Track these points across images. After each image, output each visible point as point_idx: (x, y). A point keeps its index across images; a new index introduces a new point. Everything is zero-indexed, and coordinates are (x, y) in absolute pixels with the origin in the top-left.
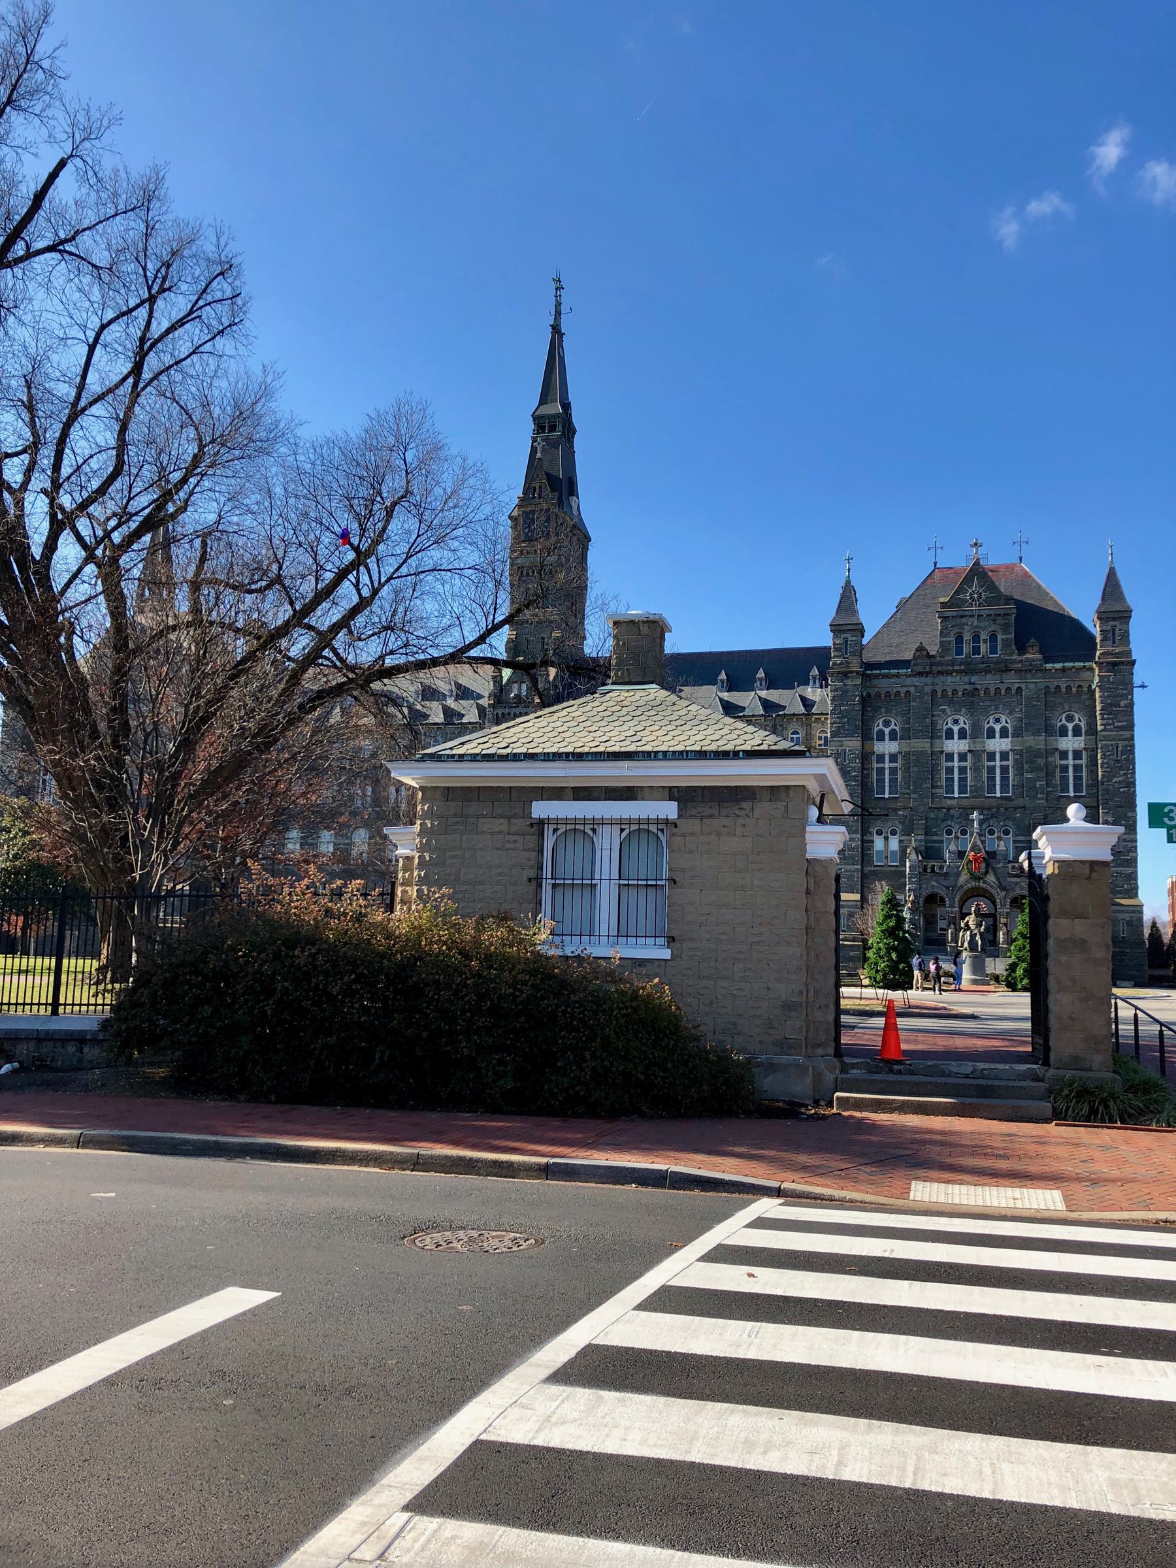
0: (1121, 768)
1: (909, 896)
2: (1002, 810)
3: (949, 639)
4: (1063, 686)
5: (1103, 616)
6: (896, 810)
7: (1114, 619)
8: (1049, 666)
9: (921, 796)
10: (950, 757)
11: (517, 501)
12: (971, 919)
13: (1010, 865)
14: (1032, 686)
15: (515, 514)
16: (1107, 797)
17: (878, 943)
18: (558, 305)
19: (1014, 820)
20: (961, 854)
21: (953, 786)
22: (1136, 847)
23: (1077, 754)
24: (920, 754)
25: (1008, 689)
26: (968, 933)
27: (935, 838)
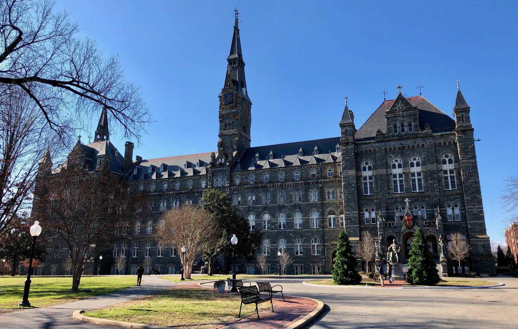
0: (472, 176)
1: (380, 237)
2: (420, 198)
3: (390, 126)
4: (442, 142)
5: (457, 111)
6: (373, 200)
7: (462, 112)
8: (435, 134)
9: (383, 194)
10: (395, 176)
11: (221, 91)
12: (393, 246)
13: (424, 222)
14: (429, 143)
15: (221, 95)
16: (467, 189)
17: (338, 260)
18: (237, 20)
19: (425, 202)
20: (402, 218)
21: (397, 188)
22: (483, 211)
23: (451, 172)
24: (381, 175)
25: (418, 146)
26: (391, 253)
27: (391, 211)
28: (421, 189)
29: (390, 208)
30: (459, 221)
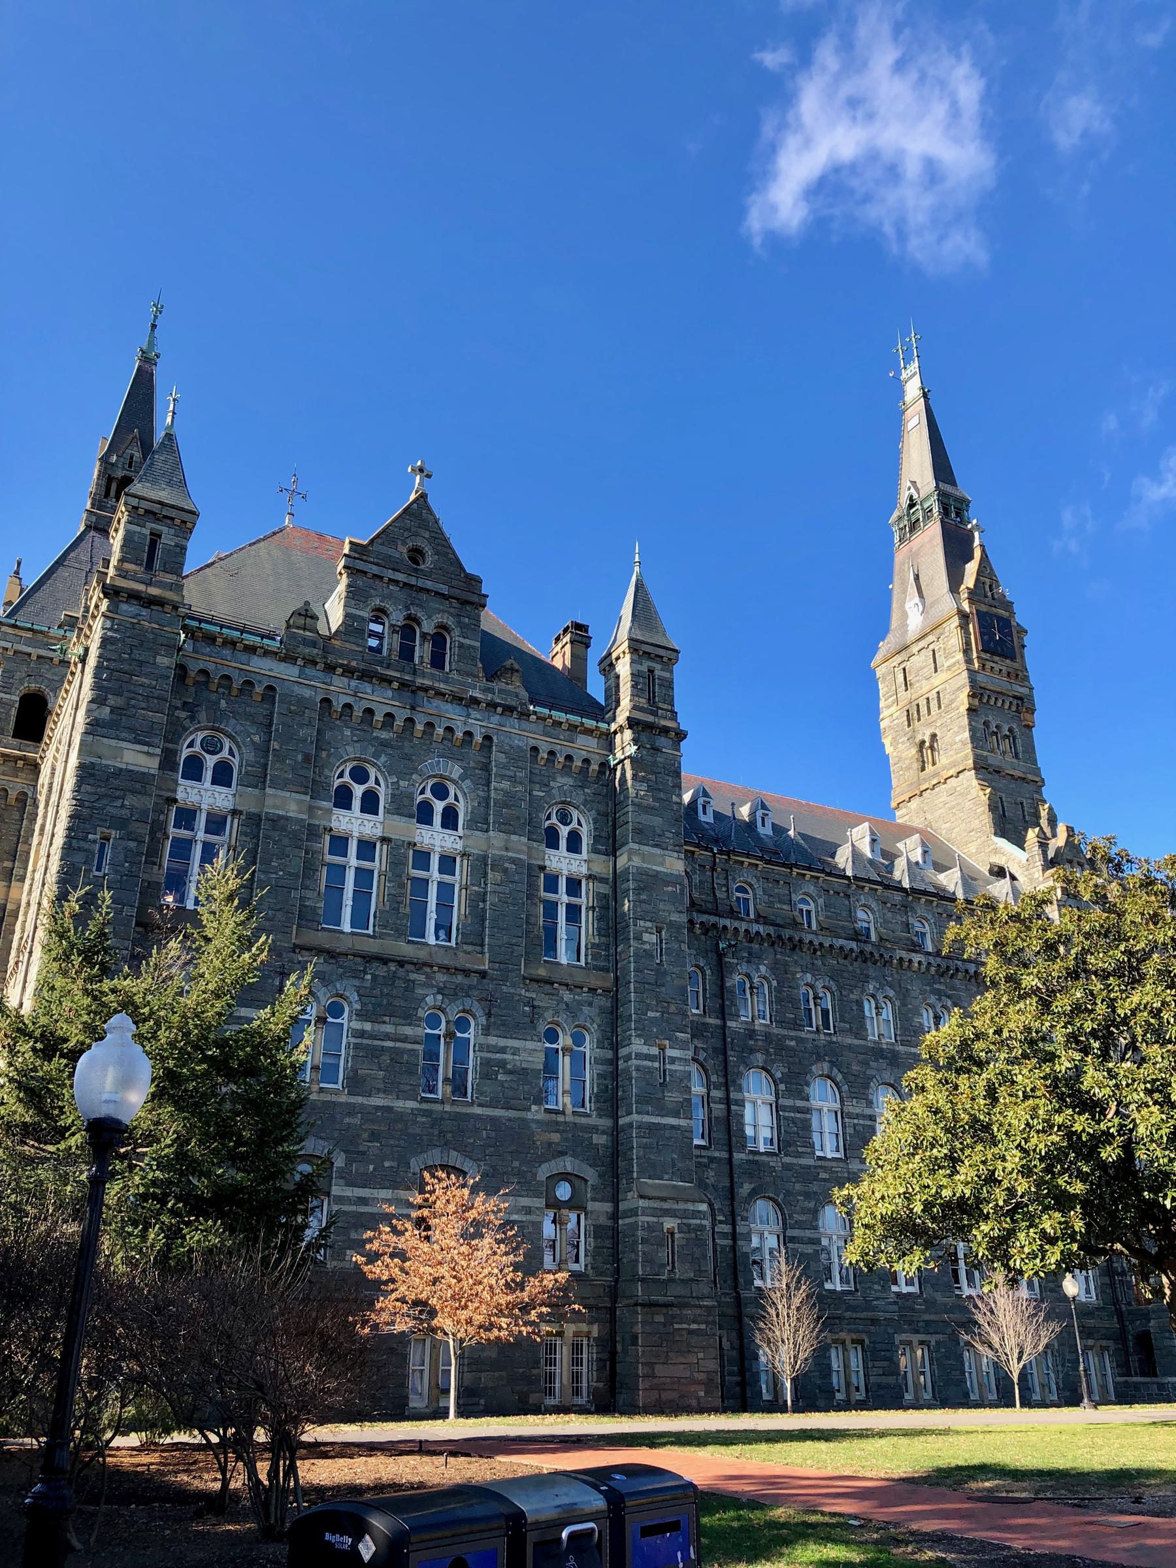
10: (340, 844)
30: (582, 1110)
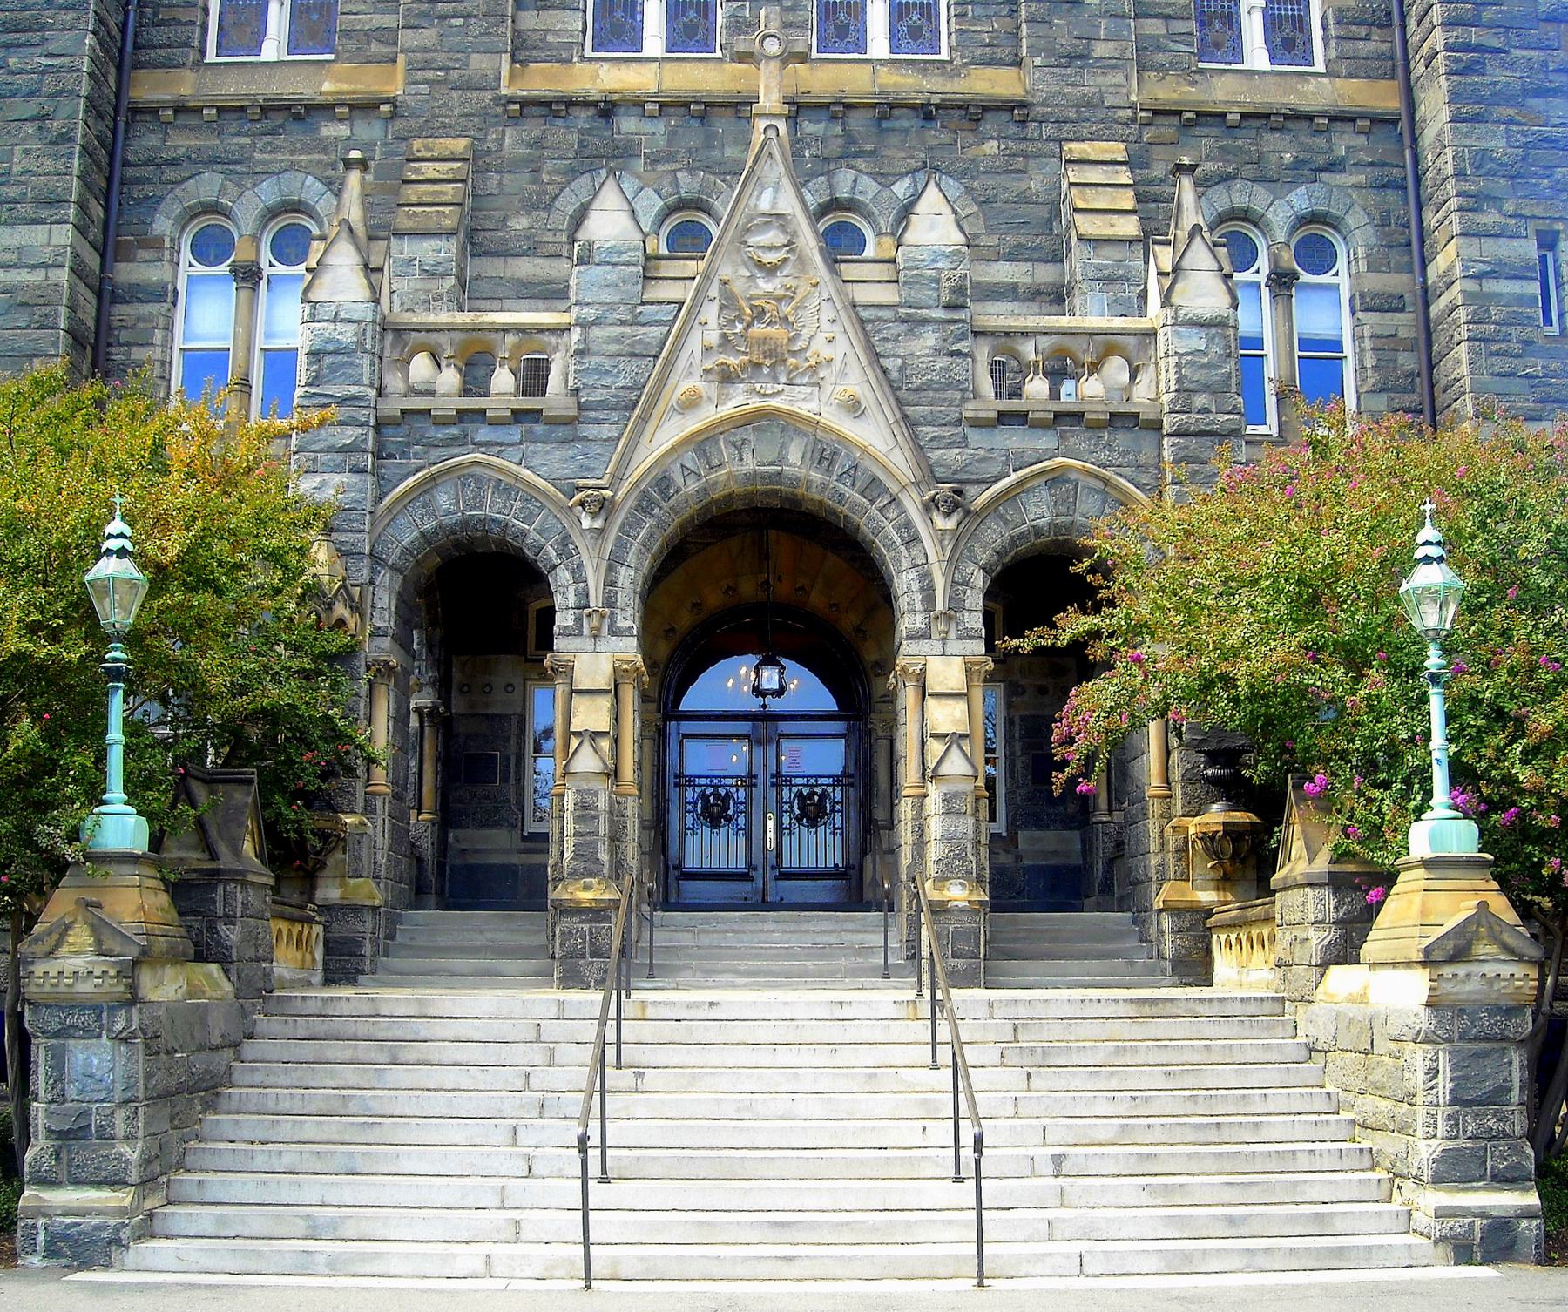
16: (1474, 36)
28: (915, 33)
29: (520, 223)
